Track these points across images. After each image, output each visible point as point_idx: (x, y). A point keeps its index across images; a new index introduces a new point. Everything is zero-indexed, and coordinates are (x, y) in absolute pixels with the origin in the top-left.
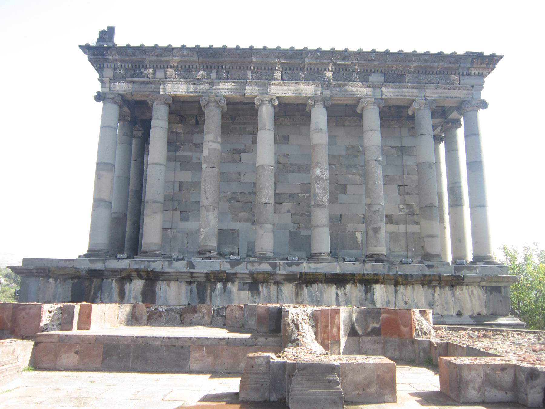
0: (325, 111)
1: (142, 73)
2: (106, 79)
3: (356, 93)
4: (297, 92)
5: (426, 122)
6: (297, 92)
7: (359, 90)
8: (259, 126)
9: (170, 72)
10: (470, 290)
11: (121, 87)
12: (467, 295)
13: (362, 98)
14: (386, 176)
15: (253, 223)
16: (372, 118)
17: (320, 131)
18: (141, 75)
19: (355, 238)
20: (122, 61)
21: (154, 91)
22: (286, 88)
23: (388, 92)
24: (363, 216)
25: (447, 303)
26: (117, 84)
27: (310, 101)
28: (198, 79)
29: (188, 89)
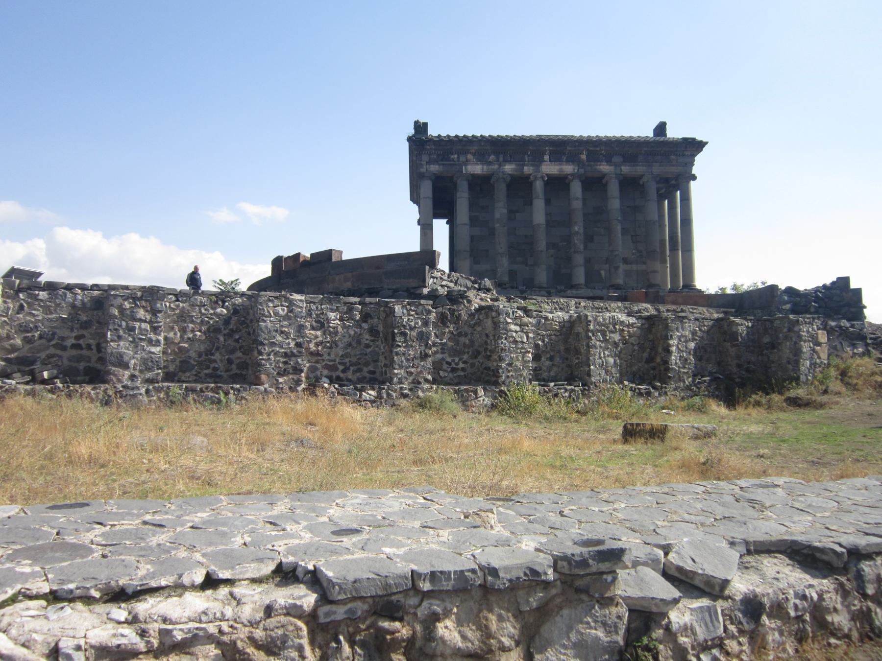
0: (580, 184)
4: (561, 170)
5: (652, 189)
6: (561, 170)
7: (605, 168)
8: (534, 196)
9: (470, 156)
11: (434, 168)
13: (606, 174)
14: (623, 229)
15: (527, 265)
16: (614, 189)
17: (577, 199)
18: (448, 159)
19: (600, 275)
20: (435, 150)
23: (625, 169)
27: (570, 177)
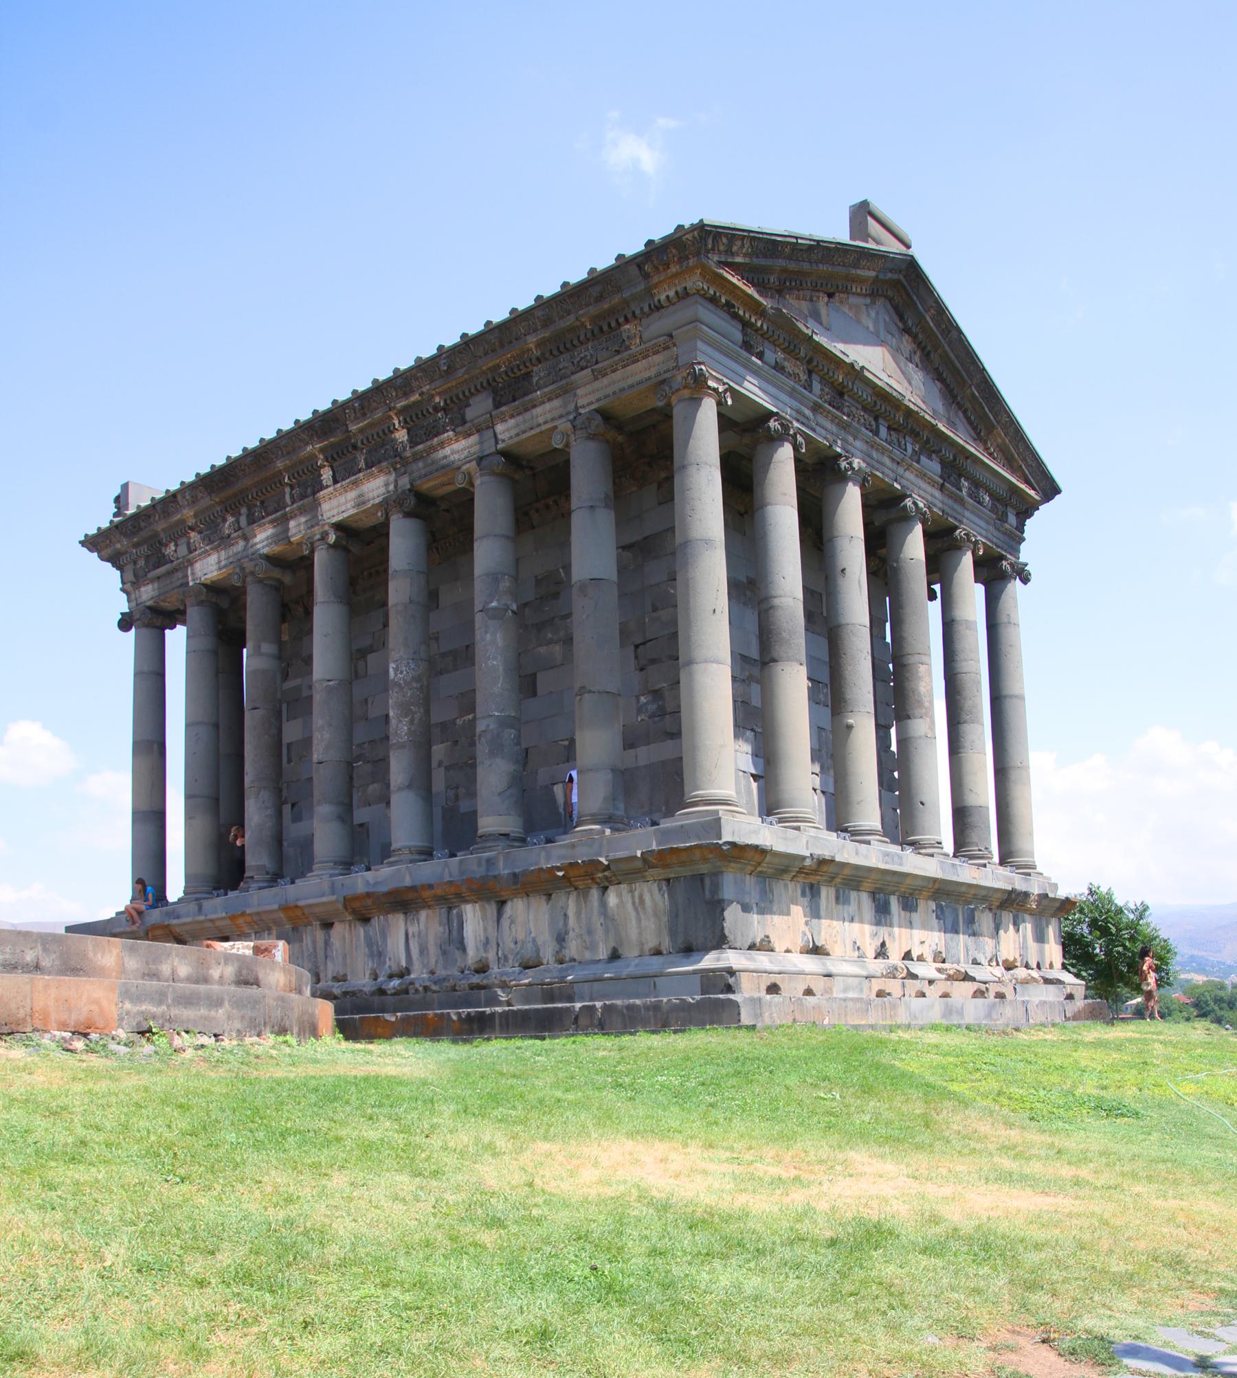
1: (164, 556)
2: (128, 586)
3: (452, 458)
6: (360, 500)
10: (636, 894)
11: (147, 593)
12: (629, 906)
18: (162, 560)
20: (136, 546)
21: (182, 585)
22: (342, 499)
23: (507, 431)
24: (566, 743)
25: (590, 932)
26: (143, 589)
28: (229, 536)
29: (219, 562)
